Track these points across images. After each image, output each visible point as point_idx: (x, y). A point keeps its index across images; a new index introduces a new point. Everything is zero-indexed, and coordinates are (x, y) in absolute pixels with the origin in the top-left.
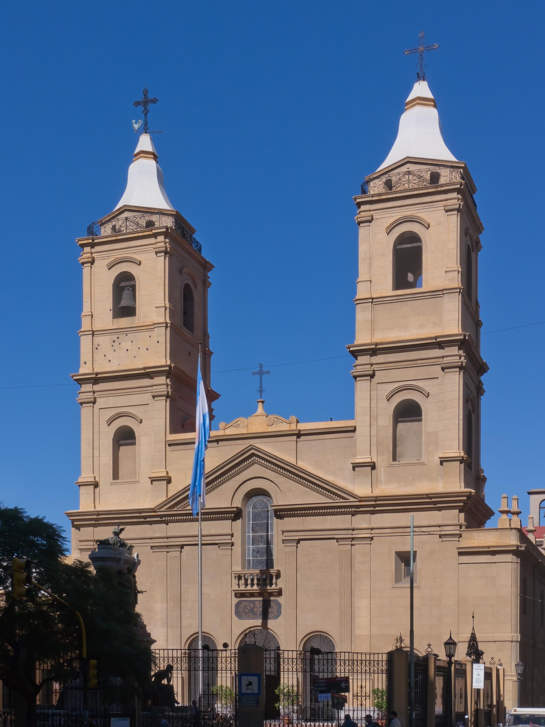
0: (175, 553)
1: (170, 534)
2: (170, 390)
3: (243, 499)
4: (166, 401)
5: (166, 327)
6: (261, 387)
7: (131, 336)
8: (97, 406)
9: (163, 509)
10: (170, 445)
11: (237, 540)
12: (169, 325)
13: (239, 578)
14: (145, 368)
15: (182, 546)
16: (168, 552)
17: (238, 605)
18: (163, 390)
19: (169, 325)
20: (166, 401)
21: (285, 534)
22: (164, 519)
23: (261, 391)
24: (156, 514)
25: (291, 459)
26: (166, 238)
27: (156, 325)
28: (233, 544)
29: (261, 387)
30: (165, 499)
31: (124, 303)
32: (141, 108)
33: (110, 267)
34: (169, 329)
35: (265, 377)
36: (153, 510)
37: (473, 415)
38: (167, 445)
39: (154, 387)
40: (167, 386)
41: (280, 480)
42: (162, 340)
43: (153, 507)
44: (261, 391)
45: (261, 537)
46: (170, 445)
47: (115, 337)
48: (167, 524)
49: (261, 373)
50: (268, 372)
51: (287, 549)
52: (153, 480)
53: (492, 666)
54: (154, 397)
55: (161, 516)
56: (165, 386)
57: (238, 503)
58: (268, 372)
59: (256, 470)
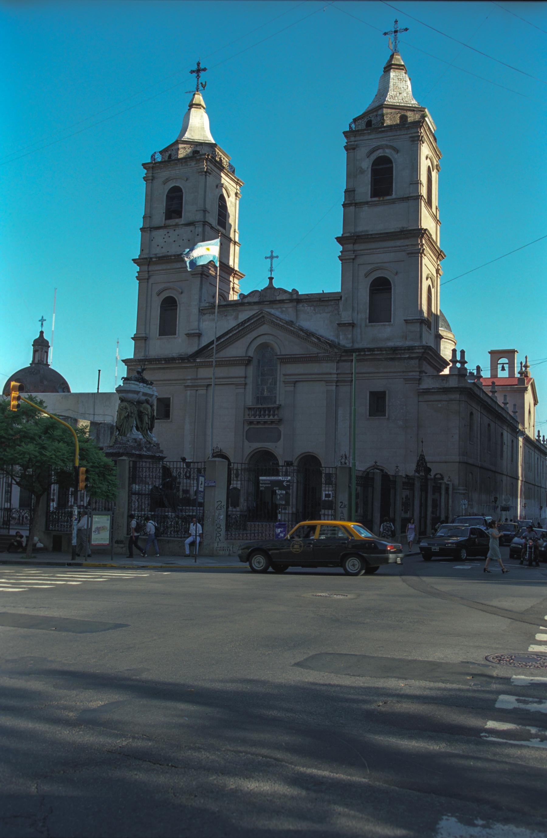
6: (271, 267)
8: (151, 281)
11: (250, 381)
16: (197, 390)
23: (271, 271)
28: (246, 384)
29: (271, 267)
32: (195, 75)
35: (275, 260)
37: (433, 290)
44: (271, 271)
49: (272, 257)
50: (277, 257)
52: (188, 335)
53: (449, 483)
57: (251, 353)
58: (277, 257)
59: (265, 329)
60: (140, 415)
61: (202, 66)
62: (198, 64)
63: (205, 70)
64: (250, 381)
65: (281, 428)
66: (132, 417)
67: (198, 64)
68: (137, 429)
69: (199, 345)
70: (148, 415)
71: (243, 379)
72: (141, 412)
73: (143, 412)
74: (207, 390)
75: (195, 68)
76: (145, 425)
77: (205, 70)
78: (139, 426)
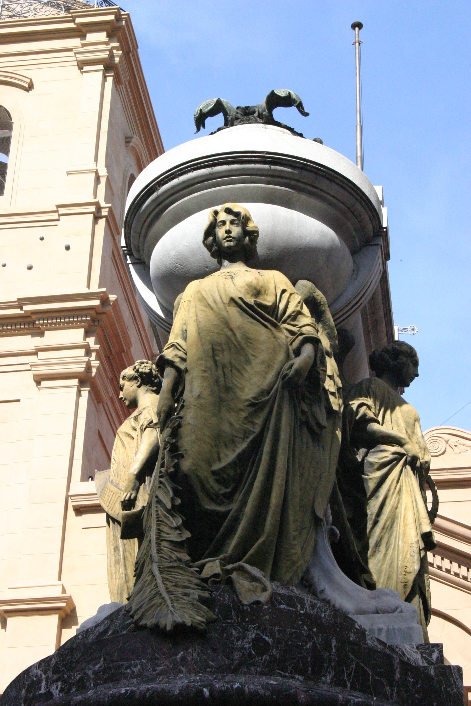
2: (96, 364)
4: (79, 394)
5: (97, 218)
12: (105, 212)
14: (21, 302)
18: (76, 361)
19: (105, 212)
20: (79, 394)
27: (63, 210)
34: (102, 222)
38: (71, 512)
39: (41, 355)
40: (88, 352)
42: (81, 246)
46: (79, 511)
54: (39, 380)
56: (82, 352)
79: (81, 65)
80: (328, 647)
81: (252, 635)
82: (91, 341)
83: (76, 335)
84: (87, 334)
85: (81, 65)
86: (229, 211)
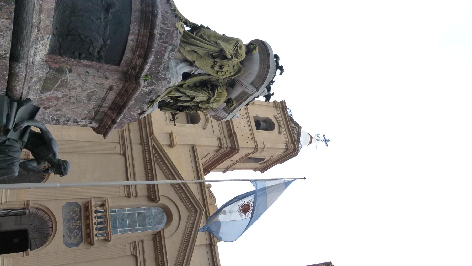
0: (118, 149)
1: (134, 146)
3: (166, 206)
7: (247, 126)
9: (153, 142)
10: (193, 148)
13: (103, 205)
15: (125, 155)
16: (119, 143)
17: (77, 205)
21: (140, 243)
22: (145, 141)
24: (149, 135)
25: (197, 243)
26: (293, 149)
30: (161, 143)
31: (262, 124)
33: (275, 117)
36: (152, 134)
40: (227, 148)
41: (180, 233)
43: (155, 133)
45: (134, 221)
47: (245, 116)
48: (141, 144)
51: (128, 246)
52: (171, 135)
55: (147, 139)
57: (163, 201)
59: (185, 213)
60: (208, 85)
61: (328, 143)
62: (329, 141)
63: (327, 145)
64: (132, 202)
65: (82, 245)
66: (213, 67)
67: (329, 141)
68: (186, 76)
69: (163, 145)
70: (208, 102)
71: (134, 195)
72: (217, 87)
73: (213, 91)
74: (120, 154)
75: (327, 139)
76: (191, 93)
77: (327, 145)
78: (190, 81)
79: (286, 144)
80: (168, 27)
81: (169, 11)
82: (228, 149)
83: (229, 145)
84: (231, 147)
85: (286, 144)
86: (256, 48)
